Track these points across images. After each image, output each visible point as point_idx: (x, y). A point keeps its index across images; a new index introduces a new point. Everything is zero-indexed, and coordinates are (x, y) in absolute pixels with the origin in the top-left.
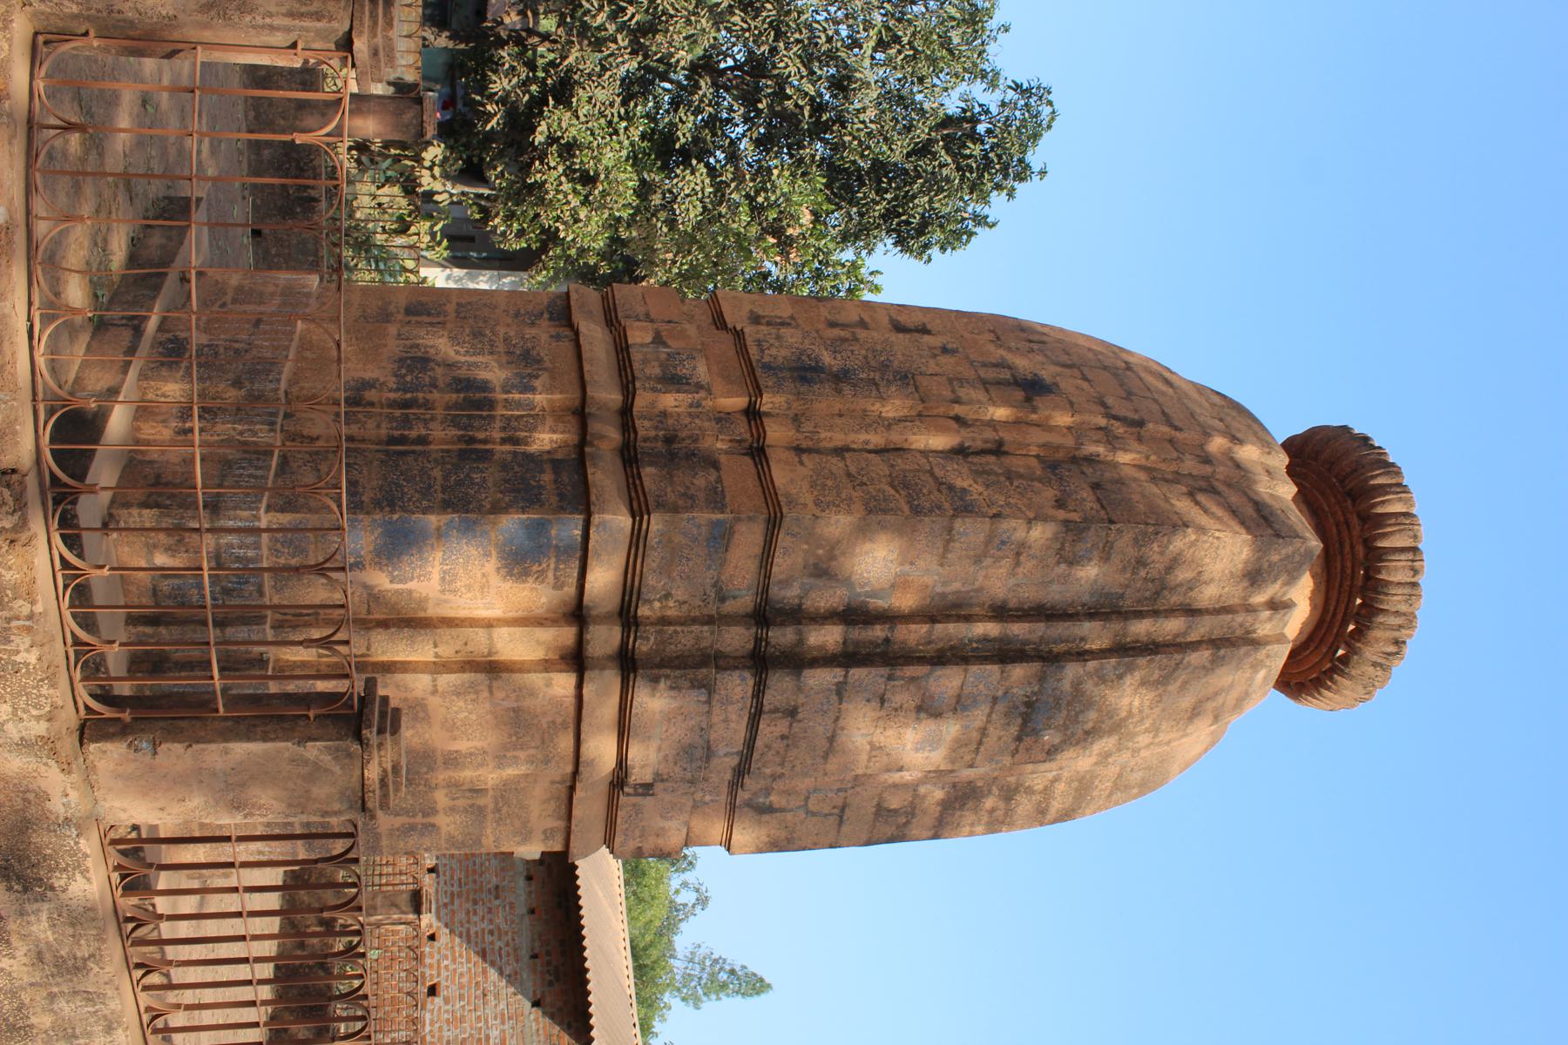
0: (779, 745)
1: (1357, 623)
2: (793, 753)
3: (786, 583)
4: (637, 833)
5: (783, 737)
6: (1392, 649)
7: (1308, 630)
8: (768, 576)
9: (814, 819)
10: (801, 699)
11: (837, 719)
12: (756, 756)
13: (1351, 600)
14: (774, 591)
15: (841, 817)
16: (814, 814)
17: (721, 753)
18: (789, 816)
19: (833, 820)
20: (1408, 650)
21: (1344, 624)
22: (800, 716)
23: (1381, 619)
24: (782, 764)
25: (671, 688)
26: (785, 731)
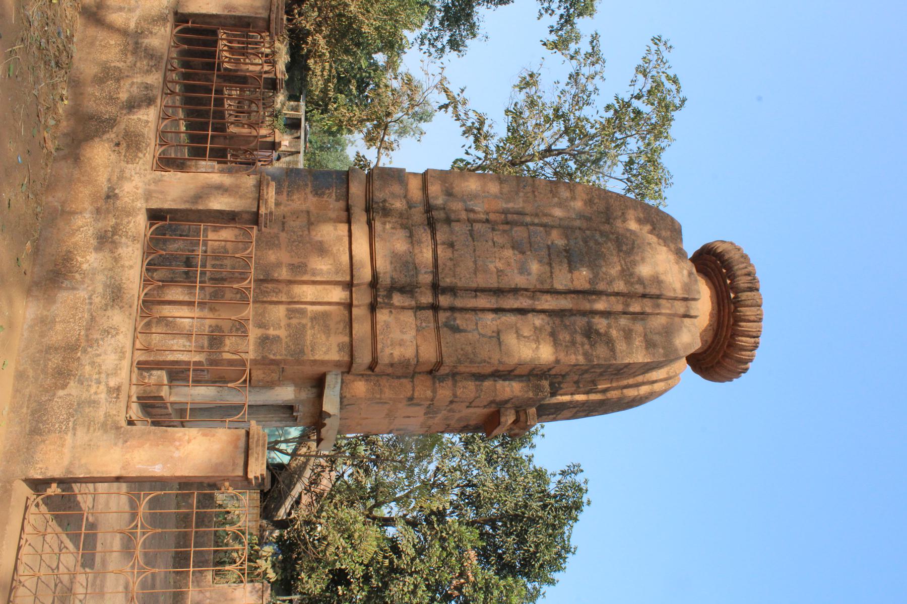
0: (449, 264)
1: (729, 278)
2: (458, 269)
3: (436, 198)
4: (389, 342)
5: (451, 259)
6: (750, 278)
7: (715, 300)
8: (427, 196)
9: (484, 339)
10: (455, 238)
11: (474, 251)
12: (440, 270)
13: (721, 272)
14: (432, 201)
15: (499, 339)
16: (483, 336)
17: (423, 272)
18: (470, 336)
19: (495, 340)
20: (758, 275)
21: (725, 282)
22: (456, 247)
23: (736, 268)
24: (454, 276)
25: (392, 228)
26: (451, 255)
